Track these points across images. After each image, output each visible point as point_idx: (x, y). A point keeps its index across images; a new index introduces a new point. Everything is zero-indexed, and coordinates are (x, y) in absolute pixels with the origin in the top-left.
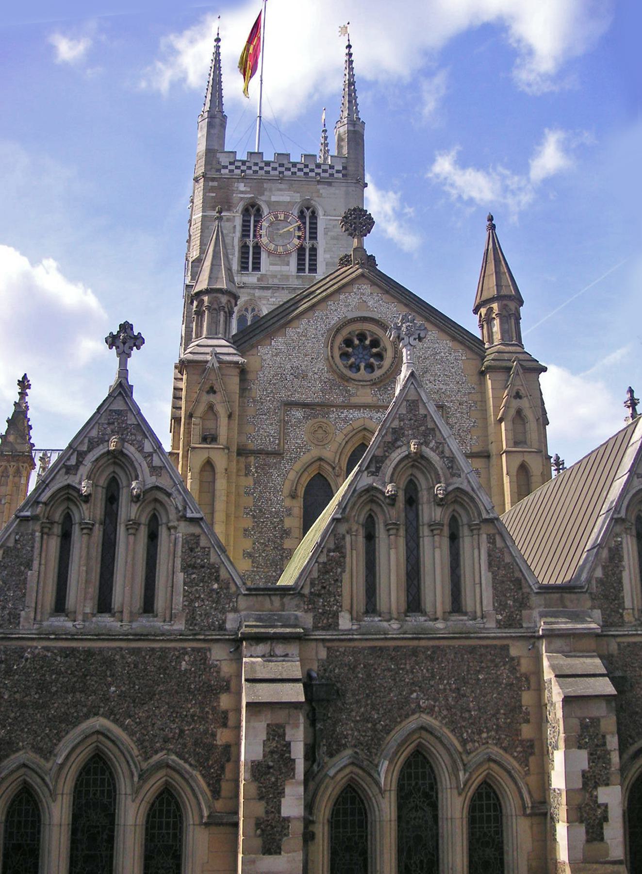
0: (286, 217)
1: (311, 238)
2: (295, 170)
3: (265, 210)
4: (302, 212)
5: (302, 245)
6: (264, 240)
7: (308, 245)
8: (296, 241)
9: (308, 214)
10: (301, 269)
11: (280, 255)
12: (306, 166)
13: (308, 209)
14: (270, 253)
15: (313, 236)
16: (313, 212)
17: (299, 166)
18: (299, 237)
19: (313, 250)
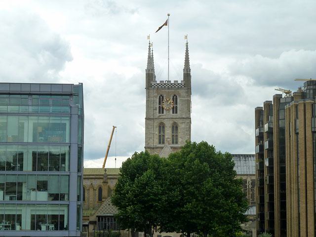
9: (175, 97)
10: (173, 113)
19: (176, 107)
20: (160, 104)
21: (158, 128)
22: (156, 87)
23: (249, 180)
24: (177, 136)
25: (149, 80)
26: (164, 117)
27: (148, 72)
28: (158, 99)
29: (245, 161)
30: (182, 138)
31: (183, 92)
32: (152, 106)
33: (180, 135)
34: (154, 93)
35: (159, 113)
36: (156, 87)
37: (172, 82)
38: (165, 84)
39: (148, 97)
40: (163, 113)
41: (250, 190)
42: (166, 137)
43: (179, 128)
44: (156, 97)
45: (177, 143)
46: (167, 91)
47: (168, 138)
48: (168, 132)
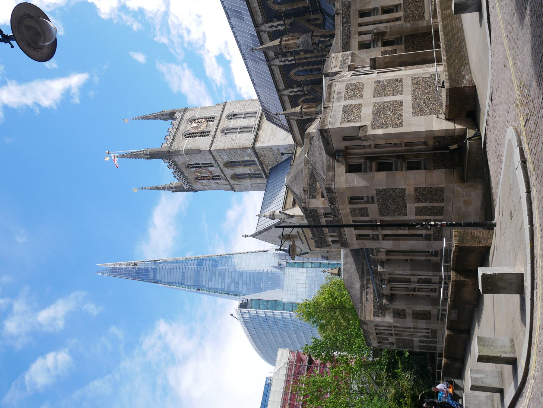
9: (191, 166)
10: (213, 166)
19: (203, 164)
24: (242, 162)
28: (203, 181)
30: (243, 157)
32: (215, 186)
33: (239, 159)
34: (197, 185)
38: (180, 177)
40: (219, 176)
41: (296, 57)
42: (249, 172)
45: (254, 161)
47: (251, 170)
48: (240, 170)
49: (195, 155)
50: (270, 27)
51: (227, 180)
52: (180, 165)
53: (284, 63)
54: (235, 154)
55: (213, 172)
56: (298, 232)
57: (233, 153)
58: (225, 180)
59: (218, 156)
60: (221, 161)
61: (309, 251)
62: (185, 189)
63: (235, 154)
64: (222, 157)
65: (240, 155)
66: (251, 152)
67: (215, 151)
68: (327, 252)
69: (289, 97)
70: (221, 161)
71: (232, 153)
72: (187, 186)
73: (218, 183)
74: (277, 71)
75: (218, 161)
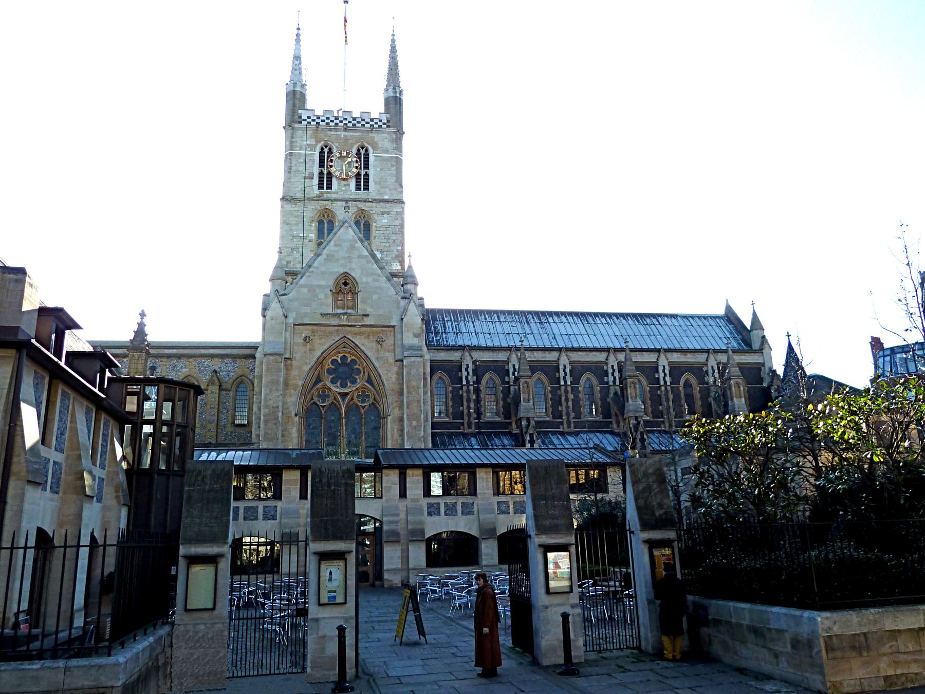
0: (348, 154)
1: (365, 168)
2: (355, 122)
3: (335, 150)
4: (359, 150)
5: (359, 172)
6: (333, 169)
7: (363, 172)
8: (355, 170)
9: (363, 152)
10: (358, 188)
11: (344, 180)
12: (363, 120)
13: (363, 148)
14: (337, 178)
15: (367, 166)
16: (366, 150)
17: (357, 120)
18: (357, 168)
19: (367, 175)
20: (321, 164)
21: (314, 225)
22: (314, 123)
23: (564, 361)
25: (294, 105)
26: (333, 196)
27: (292, 88)
29: (541, 323)
31: (383, 139)
32: (302, 168)
35: (321, 186)
36: (314, 123)
37: (354, 115)
38: (337, 118)
39: (291, 144)
40: (329, 187)
41: (569, 388)
43: (373, 229)
44: (313, 148)
46: (343, 134)
49: (395, 172)
50: (613, 366)
51: (319, 198)
52: (371, 135)
53: (561, 371)
54: (391, 241)
55: (344, 183)
56: (367, 315)
57: (394, 238)
58: (318, 196)
59: (386, 210)
60: (375, 209)
61: (291, 320)
62: (300, 111)
63: (391, 241)
64: (385, 216)
65: (386, 248)
66: (394, 268)
67: (401, 210)
68: (287, 355)
69: (507, 362)
70: (375, 209)
71: (394, 237)
72: (309, 117)
73: (312, 178)
74: (552, 356)
75: (374, 204)
